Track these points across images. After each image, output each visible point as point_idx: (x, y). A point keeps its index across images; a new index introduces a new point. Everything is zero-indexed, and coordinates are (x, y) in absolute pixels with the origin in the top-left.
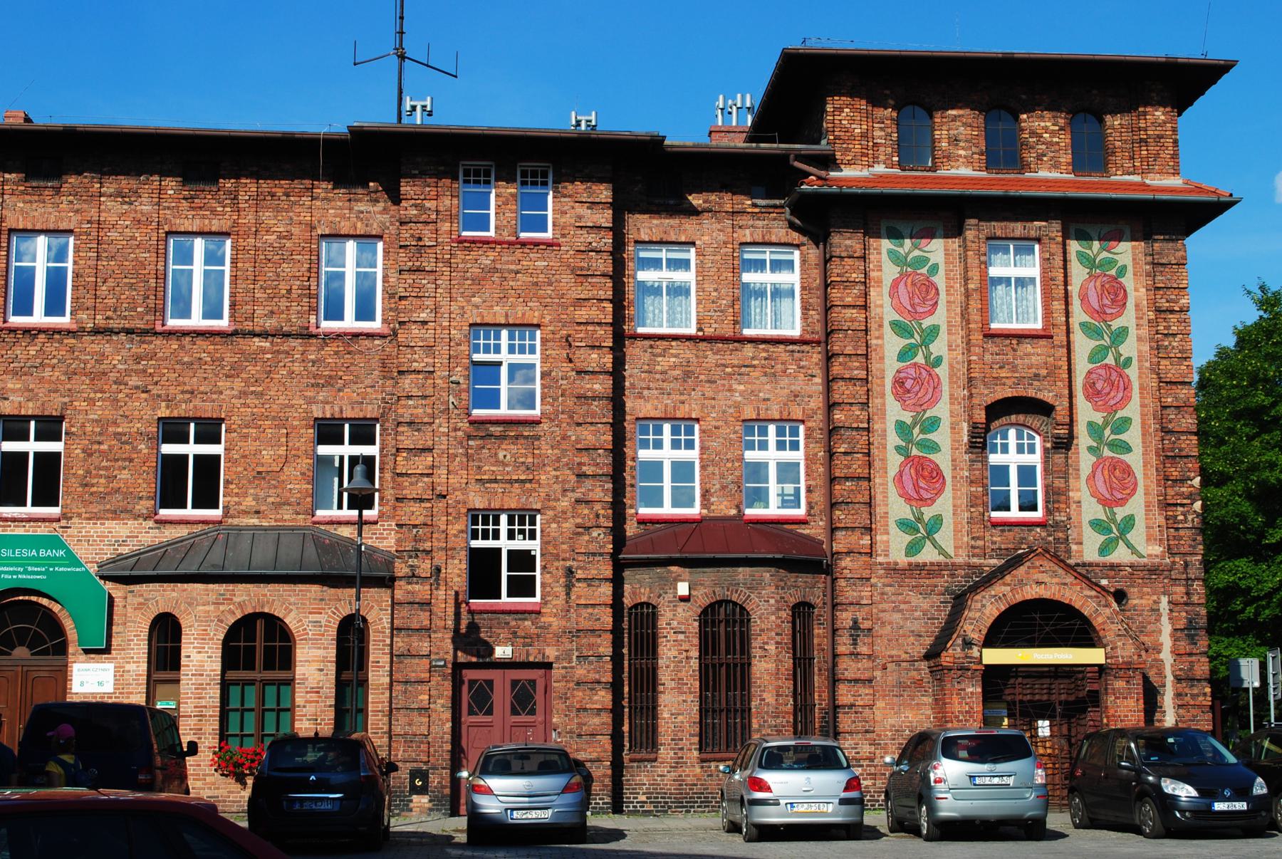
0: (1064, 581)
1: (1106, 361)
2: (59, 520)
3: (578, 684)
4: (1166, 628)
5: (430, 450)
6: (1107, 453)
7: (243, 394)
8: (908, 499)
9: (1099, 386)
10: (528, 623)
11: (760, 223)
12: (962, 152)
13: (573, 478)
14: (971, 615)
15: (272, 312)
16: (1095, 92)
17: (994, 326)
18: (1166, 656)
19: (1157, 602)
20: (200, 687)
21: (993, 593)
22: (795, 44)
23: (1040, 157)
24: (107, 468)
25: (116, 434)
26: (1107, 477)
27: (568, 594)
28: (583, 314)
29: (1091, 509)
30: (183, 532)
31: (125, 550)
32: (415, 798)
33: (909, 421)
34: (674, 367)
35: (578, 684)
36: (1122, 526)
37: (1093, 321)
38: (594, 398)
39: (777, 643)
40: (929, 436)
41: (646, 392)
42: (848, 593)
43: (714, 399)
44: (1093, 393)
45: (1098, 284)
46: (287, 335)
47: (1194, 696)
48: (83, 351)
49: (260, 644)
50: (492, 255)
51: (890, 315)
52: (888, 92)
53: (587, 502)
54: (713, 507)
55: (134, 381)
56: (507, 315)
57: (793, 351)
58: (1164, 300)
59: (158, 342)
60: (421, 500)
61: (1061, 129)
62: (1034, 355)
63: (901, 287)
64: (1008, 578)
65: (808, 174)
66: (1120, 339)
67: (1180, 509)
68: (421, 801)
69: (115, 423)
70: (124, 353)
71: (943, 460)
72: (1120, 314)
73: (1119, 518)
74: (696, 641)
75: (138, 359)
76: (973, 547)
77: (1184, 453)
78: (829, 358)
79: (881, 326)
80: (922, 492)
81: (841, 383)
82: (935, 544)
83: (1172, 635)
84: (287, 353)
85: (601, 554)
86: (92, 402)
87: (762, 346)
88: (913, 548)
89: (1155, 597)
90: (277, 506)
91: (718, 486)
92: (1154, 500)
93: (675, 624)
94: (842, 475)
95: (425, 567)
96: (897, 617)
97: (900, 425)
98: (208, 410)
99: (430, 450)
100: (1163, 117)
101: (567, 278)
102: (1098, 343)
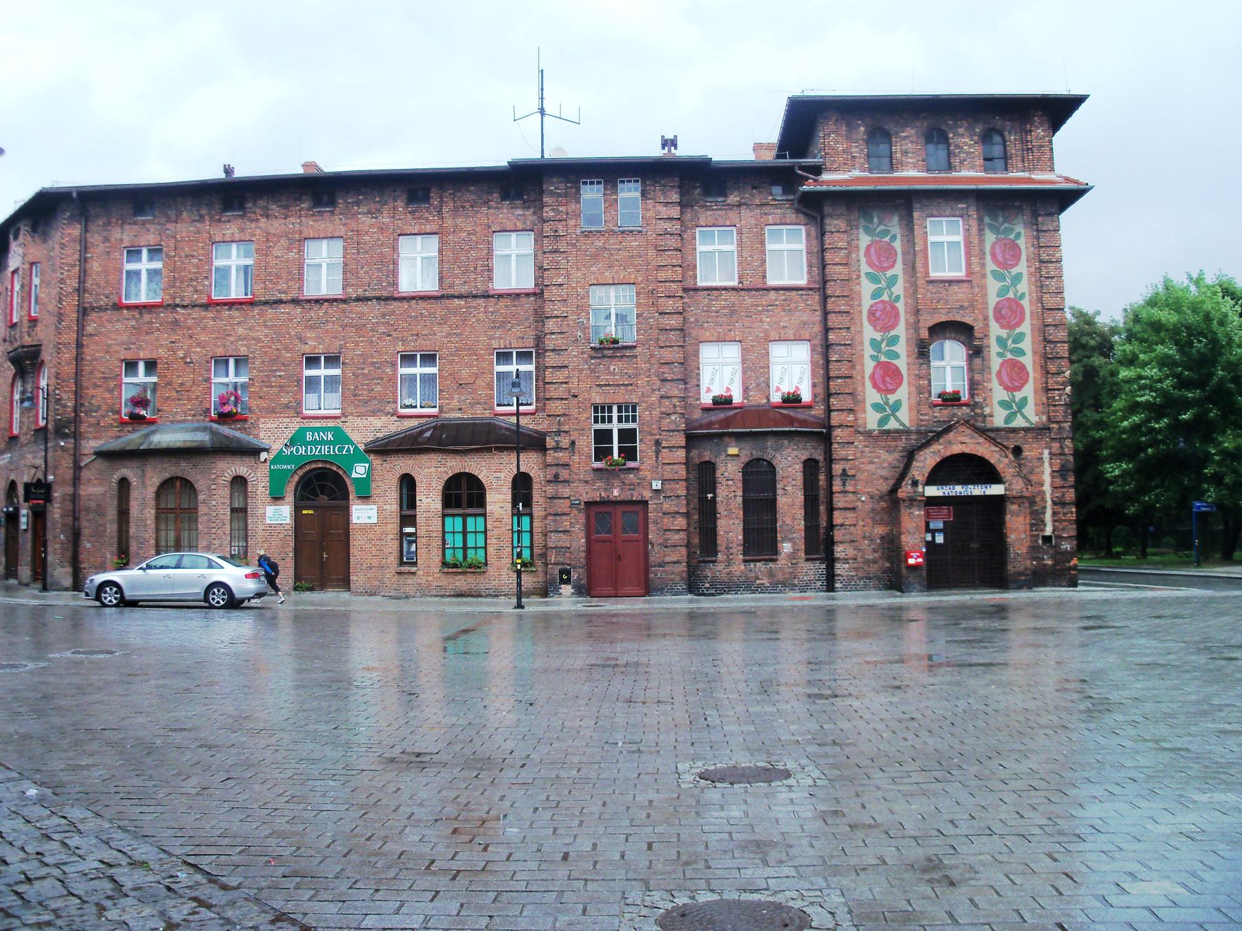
2: (339, 417)
3: (664, 514)
4: (1047, 470)
5: (566, 367)
7: (449, 335)
8: (879, 390)
9: (1003, 312)
10: (632, 476)
11: (779, 211)
12: (910, 160)
13: (659, 383)
14: (918, 465)
15: (465, 282)
17: (934, 275)
18: (1047, 488)
19: (1042, 454)
20: (427, 519)
22: (797, 92)
23: (961, 162)
24: (367, 385)
25: (372, 363)
27: (657, 457)
28: (662, 275)
29: (999, 393)
30: (415, 423)
31: (380, 435)
32: (563, 586)
35: (664, 514)
38: (671, 330)
40: (892, 348)
42: (838, 451)
44: (999, 317)
46: (475, 297)
47: (1065, 514)
48: (351, 312)
49: (464, 492)
50: (603, 239)
51: (865, 268)
53: (668, 397)
55: (382, 329)
56: (613, 278)
59: (396, 304)
60: (562, 399)
61: (976, 143)
63: (873, 249)
64: (941, 440)
65: (808, 178)
68: (567, 590)
69: (372, 357)
70: (376, 312)
71: (902, 364)
72: (1016, 264)
73: (1017, 399)
74: (740, 485)
75: (384, 316)
76: (921, 420)
78: (825, 298)
79: (859, 276)
81: (833, 315)
82: (897, 420)
84: (475, 307)
85: (678, 431)
86: (357, 344)
88: (883, 421)
90: (472, 405)
92: (1040, 386)
93: (726, 474)
95: (565, 441)
96: (871, 467)
97: (873, 341)
98: (426, 345)
99: (566, 367)
101: (651, 252)
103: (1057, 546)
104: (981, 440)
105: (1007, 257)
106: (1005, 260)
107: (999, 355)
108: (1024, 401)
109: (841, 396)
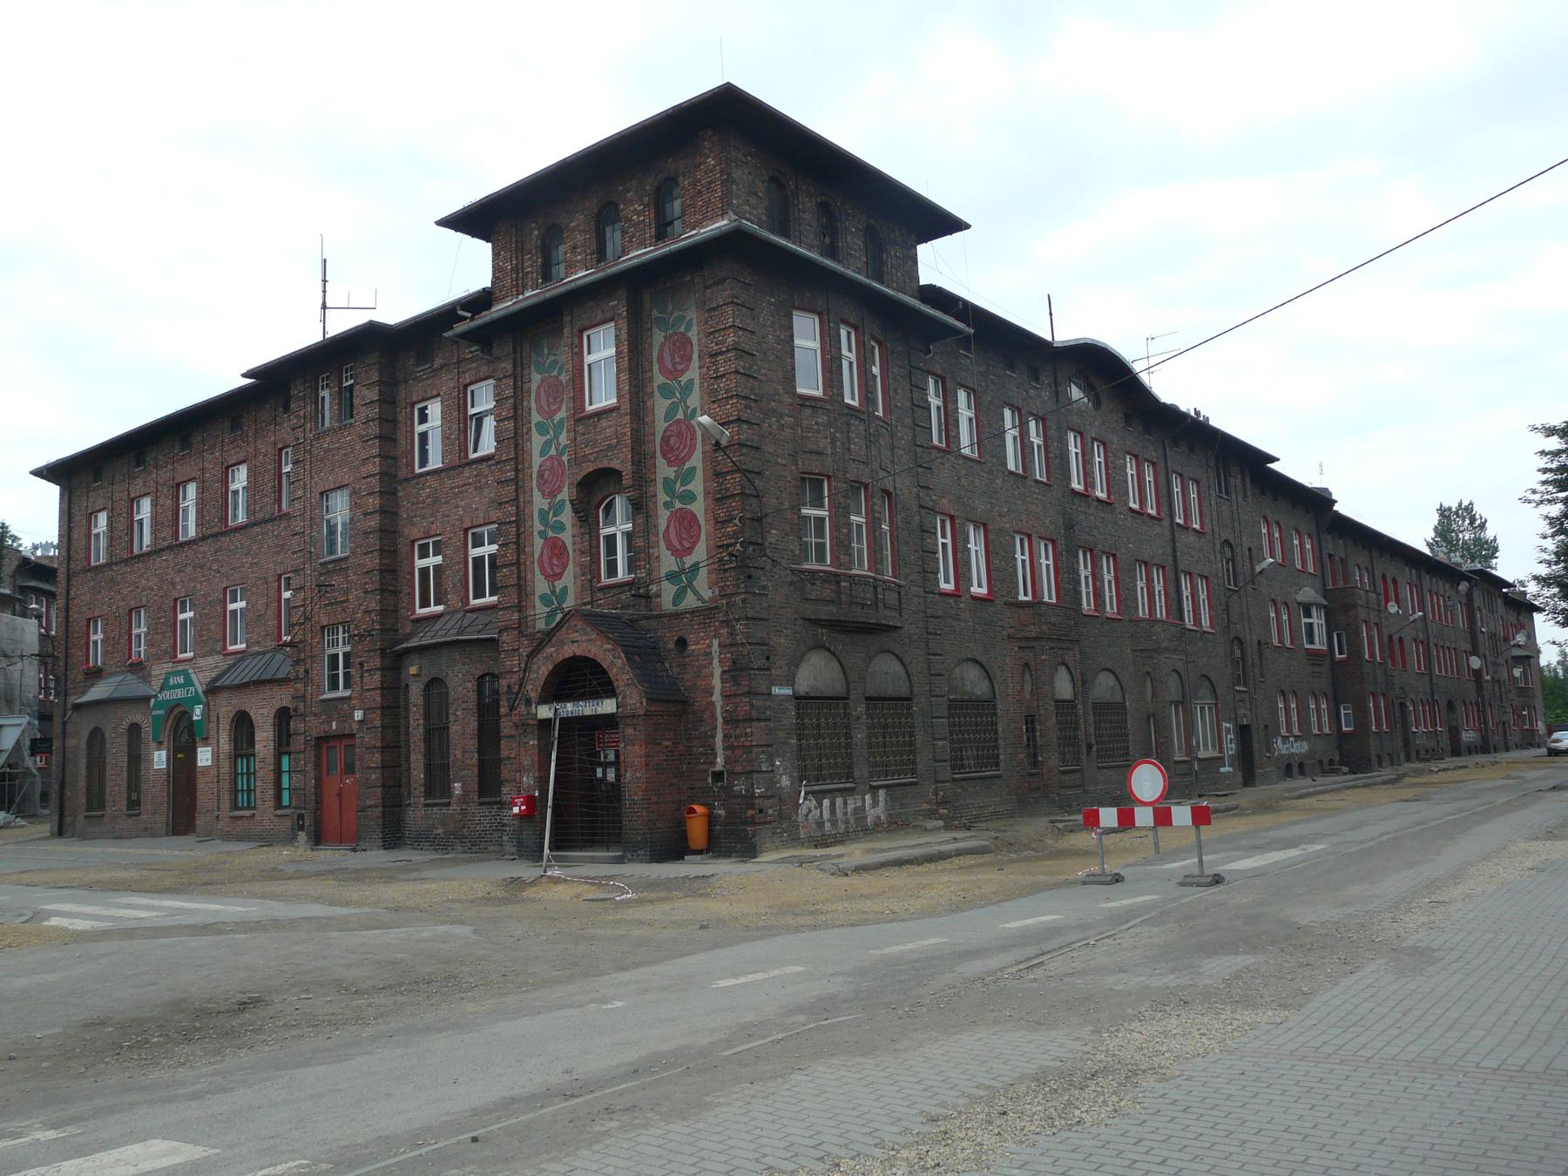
0: (590, 637)
1: (678, 417)
6: (678, 505)
7: (252, 565)
8: (547, 576)
9: (672, 442)
12: (579, 257)
16: (670, 160)
18: (717, 697)
19: (710, 646)
28: (365, 470)
33: (546, 508)
34: (428, 497)
38: (370, 532)
39: (464, 709)
40: (558, 518)
52: (533, 225)
71: (567, 537)
77: (729, 494)
83: (721, 679)
89: (708, 641)
100: (713, 163)
102: (671, 401)
103: (730, 787)
105: (677, 360)
106: (674, 364)
107: (667, 505)
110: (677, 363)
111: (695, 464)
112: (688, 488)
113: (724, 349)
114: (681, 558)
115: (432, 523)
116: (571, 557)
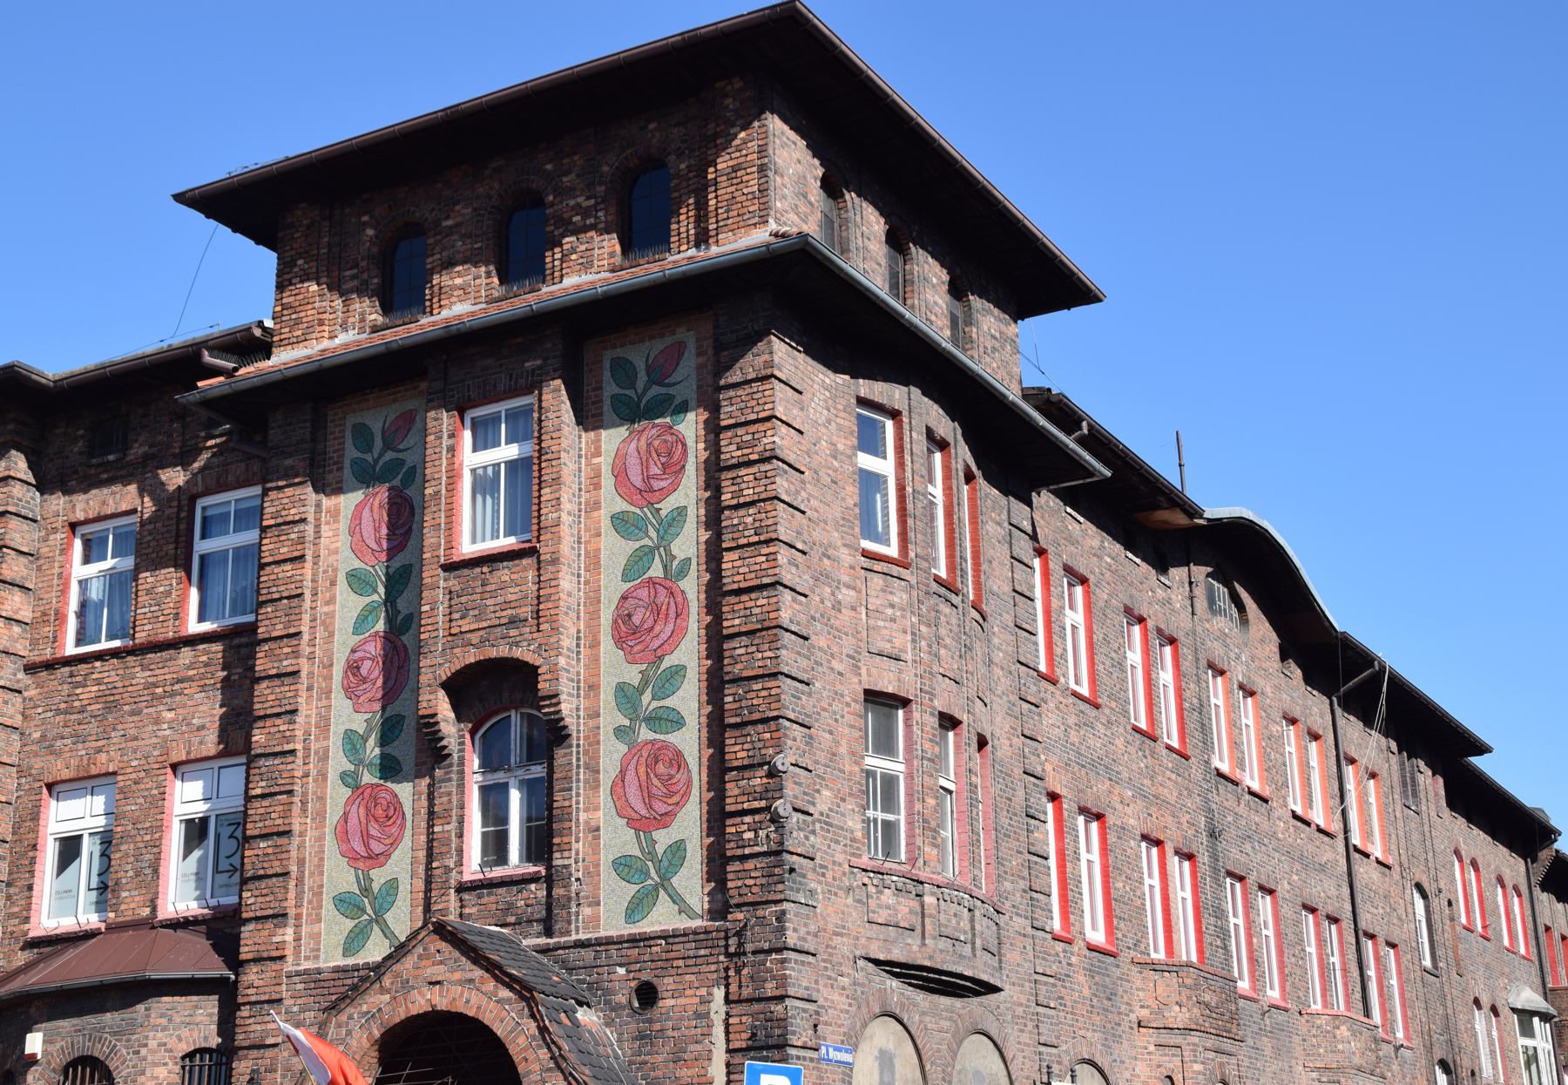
0: (469, 975)
6: (645, 734)
8: (353, 858)
16: (652, 126)
19: (706, 1001)
21: (365, 1008)
26: (643, 778)
36: (665, 863)
37: (633, 509)
41: (59, 743)
43: (136, 739)
45: (643, 443)
52: (365, 218)
54: (123, 907)
57: (239, 646)
58: (733, 447)
62: (517, 580)
64: (387, 981)
66: (672, 530)
67: (748, 819)
72: (674, 488)
77: (756, 716)
80: (372, 842)
87: (201, 647)
89: (703, 991)
91: (131, 873)
94: (256, 832)
102: (638, 545)
104: (478, 973)
105: (655, 470)
106: (648, 478)
108: (678, 850)
109: (263, 884)
110: (655, 477)
111: (684, 661)
112: (668, 702)
113: (754, 457)
114: (648, 832)
115: (99, 750)
116: (409, 824)
